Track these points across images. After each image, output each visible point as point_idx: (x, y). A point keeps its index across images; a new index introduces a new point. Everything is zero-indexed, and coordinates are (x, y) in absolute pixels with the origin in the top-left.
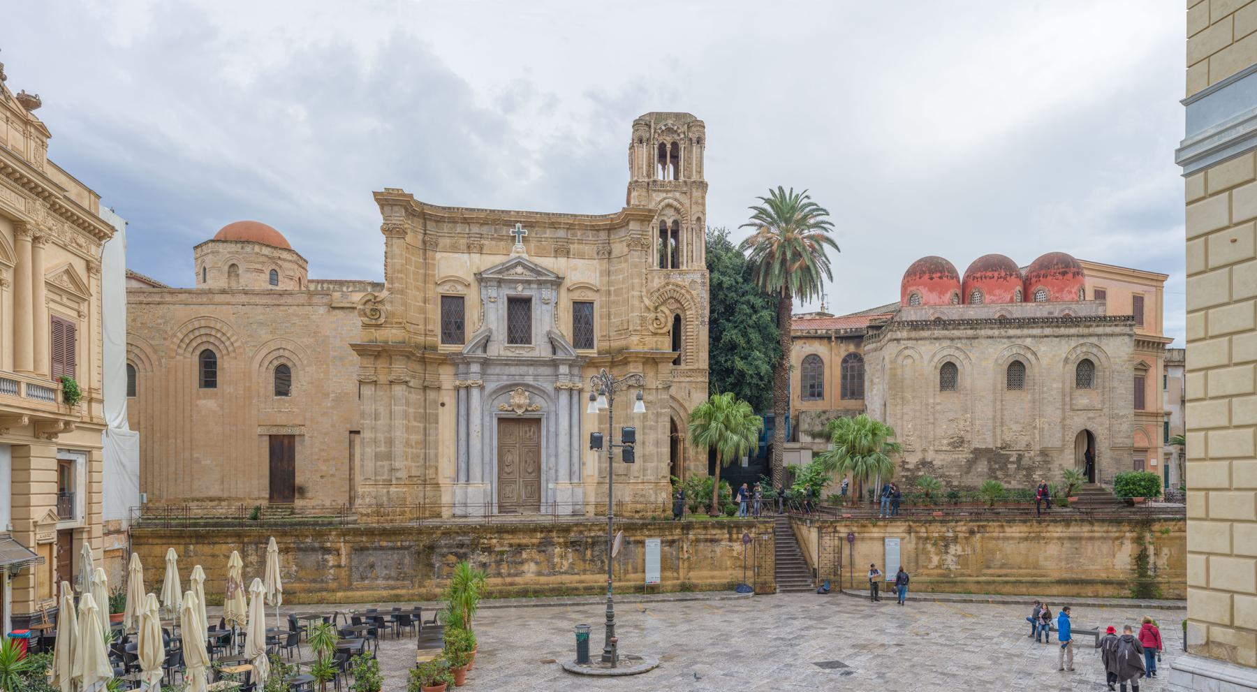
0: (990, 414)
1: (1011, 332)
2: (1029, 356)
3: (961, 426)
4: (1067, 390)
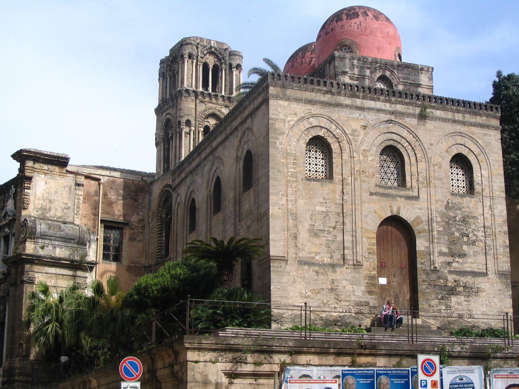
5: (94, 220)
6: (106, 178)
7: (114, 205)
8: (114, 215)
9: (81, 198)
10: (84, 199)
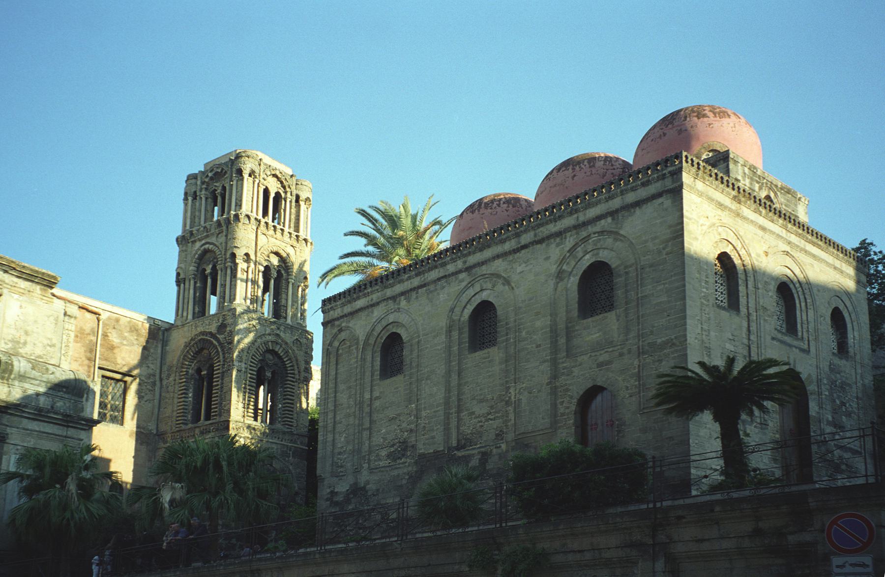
0: (440, 396)
1: (472, 260)
2: (500, 287)
3: (404, 425)
4: (561, 326)
5: (89, 367)
6: (107, 314)
7: (116, 351)
8: (116, 364)
9: (72, 335)
10: (76, 336)
